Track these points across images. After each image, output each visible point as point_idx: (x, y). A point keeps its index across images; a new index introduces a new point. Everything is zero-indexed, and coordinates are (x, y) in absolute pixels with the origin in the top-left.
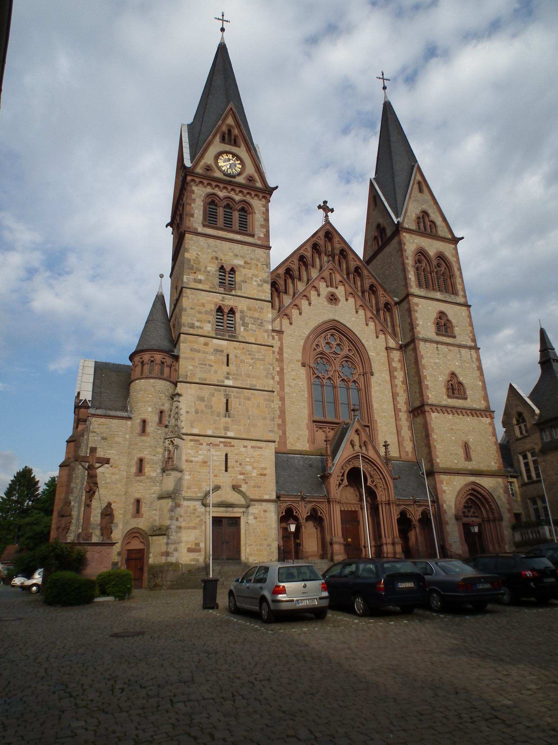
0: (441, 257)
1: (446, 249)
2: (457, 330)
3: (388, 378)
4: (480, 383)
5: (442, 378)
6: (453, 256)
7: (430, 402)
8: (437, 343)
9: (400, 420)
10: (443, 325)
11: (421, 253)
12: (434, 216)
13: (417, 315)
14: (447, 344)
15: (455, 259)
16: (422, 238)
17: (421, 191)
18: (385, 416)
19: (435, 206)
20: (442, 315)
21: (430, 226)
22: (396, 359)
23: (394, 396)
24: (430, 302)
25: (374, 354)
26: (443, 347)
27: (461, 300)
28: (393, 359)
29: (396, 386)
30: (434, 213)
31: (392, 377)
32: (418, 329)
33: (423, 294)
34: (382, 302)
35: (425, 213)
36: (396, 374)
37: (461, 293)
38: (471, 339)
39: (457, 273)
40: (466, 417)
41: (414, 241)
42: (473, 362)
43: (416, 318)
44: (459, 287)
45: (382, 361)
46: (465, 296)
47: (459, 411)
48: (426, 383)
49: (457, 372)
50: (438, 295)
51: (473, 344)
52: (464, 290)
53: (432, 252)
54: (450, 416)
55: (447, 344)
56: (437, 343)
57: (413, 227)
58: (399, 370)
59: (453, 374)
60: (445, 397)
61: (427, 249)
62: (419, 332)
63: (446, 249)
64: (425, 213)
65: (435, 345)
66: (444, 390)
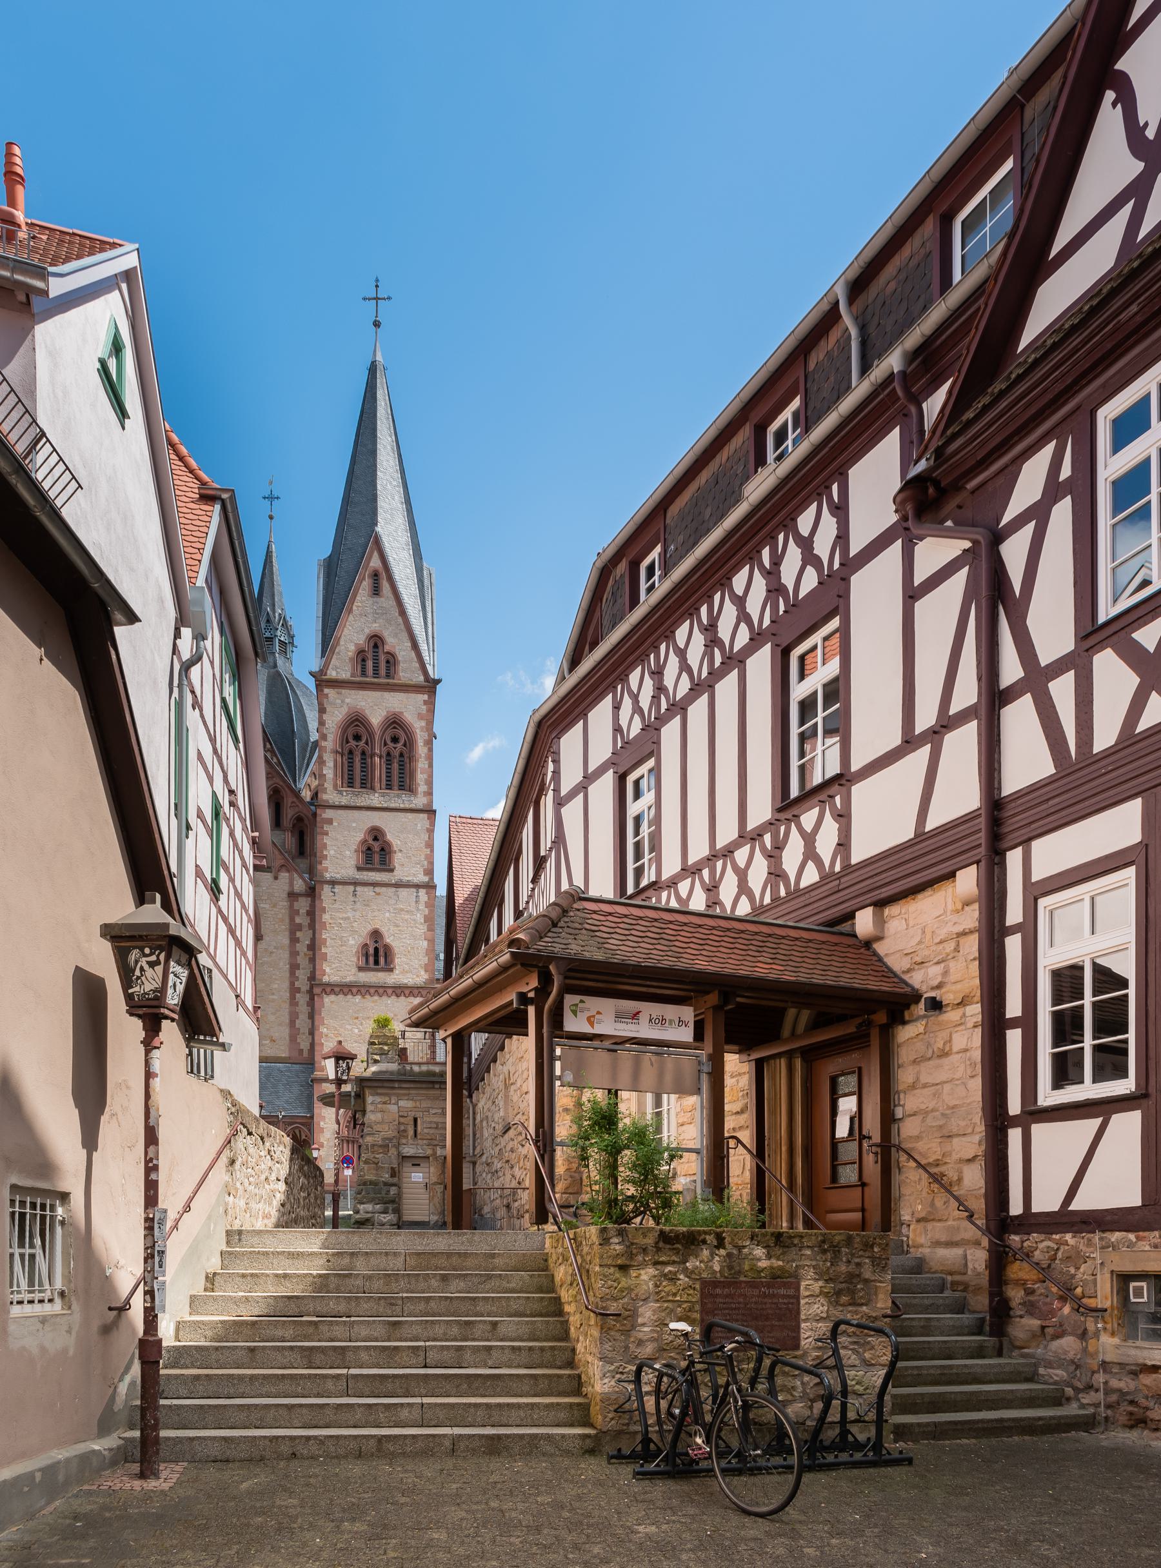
0: (395, 723)
1: (408, 706)
2: (398, 859)
3: (286, 941)
4: (425, 943)
5: (354, 942)
6: (420, 717)
7: (326, 979)
8: (355, 884)
9: (297, 1004)
10: (376, 852)
11: (355, 727)
12: (396, 643)
13: (326, 840)
14: (374, 885)
15: (423, 723)
16: (361, 692)
17: (376, 591)
18: (273, 1000)
19: (400, 620)
20: (376, 834)
21: (388, 662)
22: (303, 911)
23: (294, 967)
24: (356, 813)
25: (267, 906)
26: (366, 889)
27: (419, 801)
28: (297, 912)
29: (298, 953)
30: (396, 635)
31: (294, 940)
32: (325, 864)
33: (344, 800)
34: (289, 816)
35: (376, 641)
36: (298, 934)
37: (422, 788)
38: (425, 870)
39: (421, 749)
40: (384, 998)
41: (343, 701)
42: (418, 910)
43: (325, 846)
44: (420, 777)
45: (280, 916)
46: (429, 793)
47: (372, 991)
48: (324, 950)
49: (383, 930)
50: (375, 799)
51: (426, 879)
52: (429, 783)
53: (376, 719)
54: (358, 998)
55: (374, 885)
56: (355, 884)
57: (345, 674)
58: (305, 929)
59: (376, 935)
60: (354, 970)
61: (368, 713)
62: (326, 869)
63: (408, 706)
64: (376, 641)
65: (352, 888)
66: (355, 959)
